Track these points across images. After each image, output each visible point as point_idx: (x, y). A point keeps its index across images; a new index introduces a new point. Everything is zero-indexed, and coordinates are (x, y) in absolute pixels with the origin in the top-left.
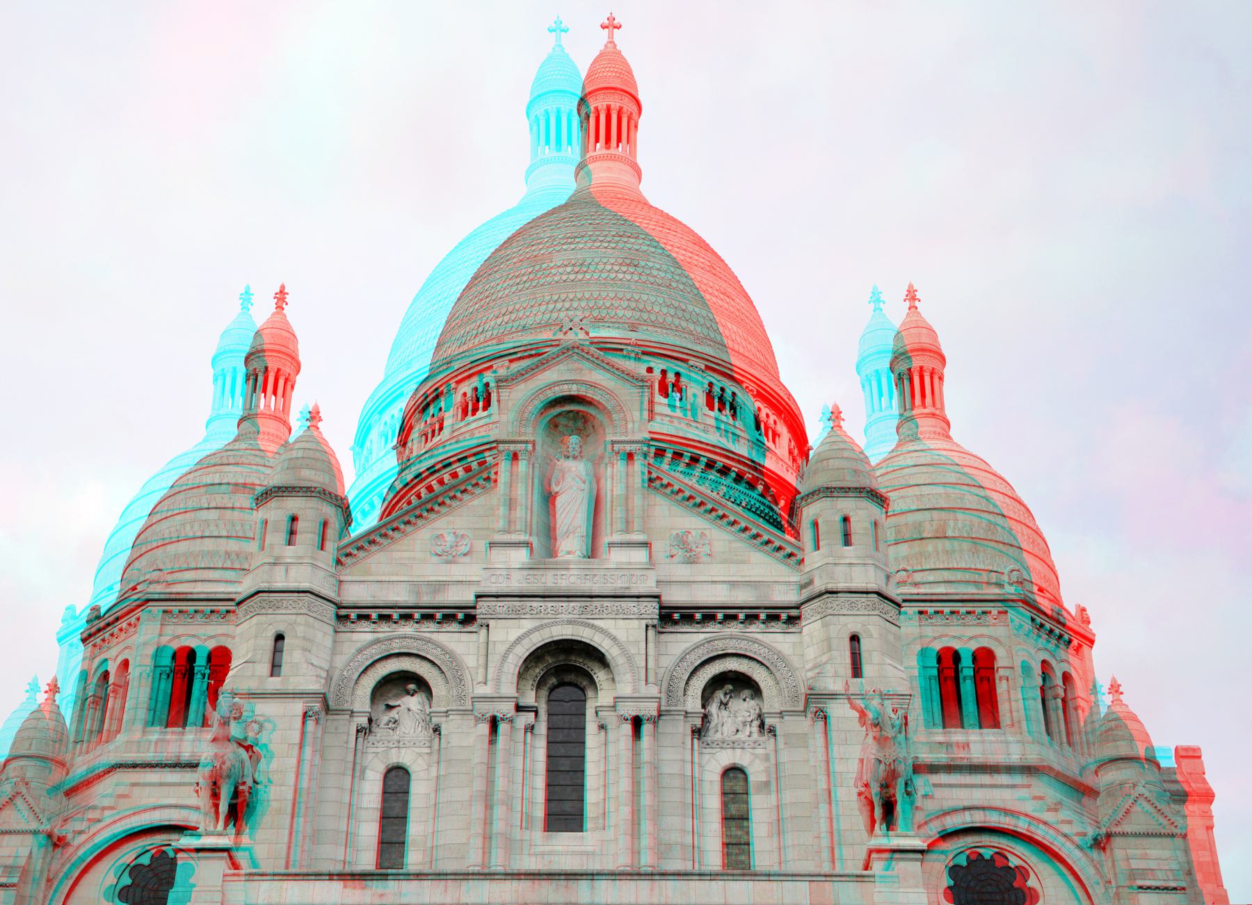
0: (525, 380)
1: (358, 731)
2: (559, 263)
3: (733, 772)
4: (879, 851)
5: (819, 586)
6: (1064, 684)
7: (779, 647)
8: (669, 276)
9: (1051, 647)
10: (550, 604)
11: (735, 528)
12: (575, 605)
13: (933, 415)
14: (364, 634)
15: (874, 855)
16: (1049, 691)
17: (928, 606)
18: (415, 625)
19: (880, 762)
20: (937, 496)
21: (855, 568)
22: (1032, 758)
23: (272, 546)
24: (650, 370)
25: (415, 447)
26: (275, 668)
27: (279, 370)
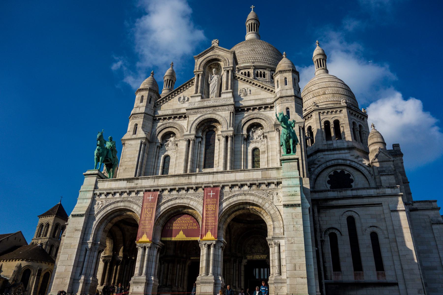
0: (201, 57)
1: (157, 147)
7: (268, 115)
9: (356, 119)
10: (205, 110)
11: (257, 86)
12: (211, 109)
13: (323, 69)
15: (282, 161)
16: (355, 130)
18: (173, 120)
19: (285, 134)
20: (323, 85)
21: (288, 90)
22: (350, 146)
24: (257, 72)
27: (170, 79)
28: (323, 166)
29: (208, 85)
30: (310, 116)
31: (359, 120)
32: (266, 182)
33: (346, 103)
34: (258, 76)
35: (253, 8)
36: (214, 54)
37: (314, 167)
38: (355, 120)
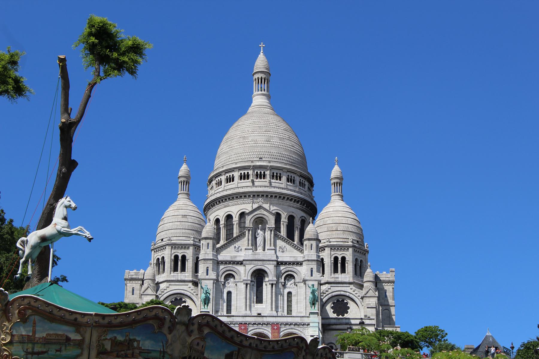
3: (289, 293)
4: (311, 313)
5: (306, 258)
6: (361, 262)
8: (278, 144)
10: (256, 262)
13: (339, 195)
14: (221, 267)
17: (333, 248)
20: (337, 220)
24: (273, 173)
25: (214, 187)
26: (207, 274)
28: (330, 295)
31: (361, 256)
32: (302, 324)
33: (352, 242)
37: (323, 296)
38: (358, 256)
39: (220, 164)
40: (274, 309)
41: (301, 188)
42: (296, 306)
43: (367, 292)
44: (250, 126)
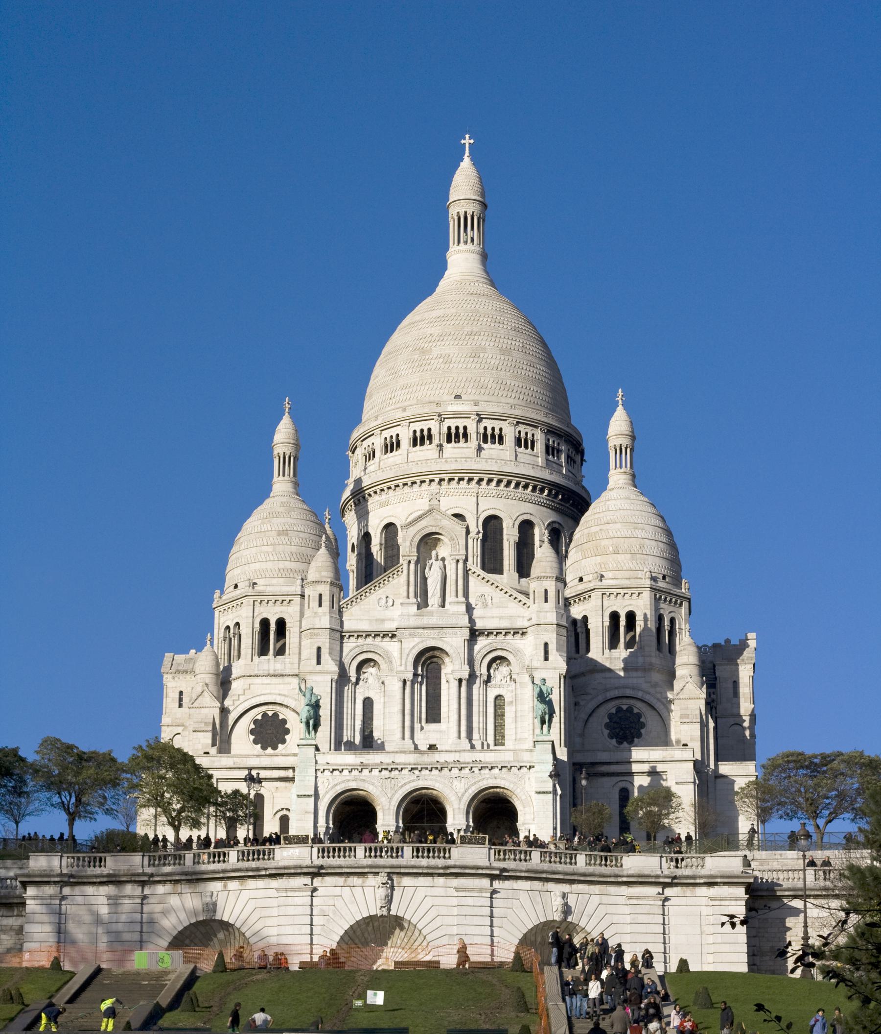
2: (435, 356)
5: (534, 622)
10: (425, 631)
12: (436, 631)
23: (313, 608)
24: (485, 428)
25: (360, 461)
26: (319, 663)
28: (601, 699)
29: (426, 579)
30: (587, 597)
31: (672, 609)
34: (485, 441)
35: (470, 143)
36: (433, 523)
39: (372, 411)
40: (464, 734)
41: (551, 457)
42: (513, 726)
43: (682, 689)
44: (436, 324)
